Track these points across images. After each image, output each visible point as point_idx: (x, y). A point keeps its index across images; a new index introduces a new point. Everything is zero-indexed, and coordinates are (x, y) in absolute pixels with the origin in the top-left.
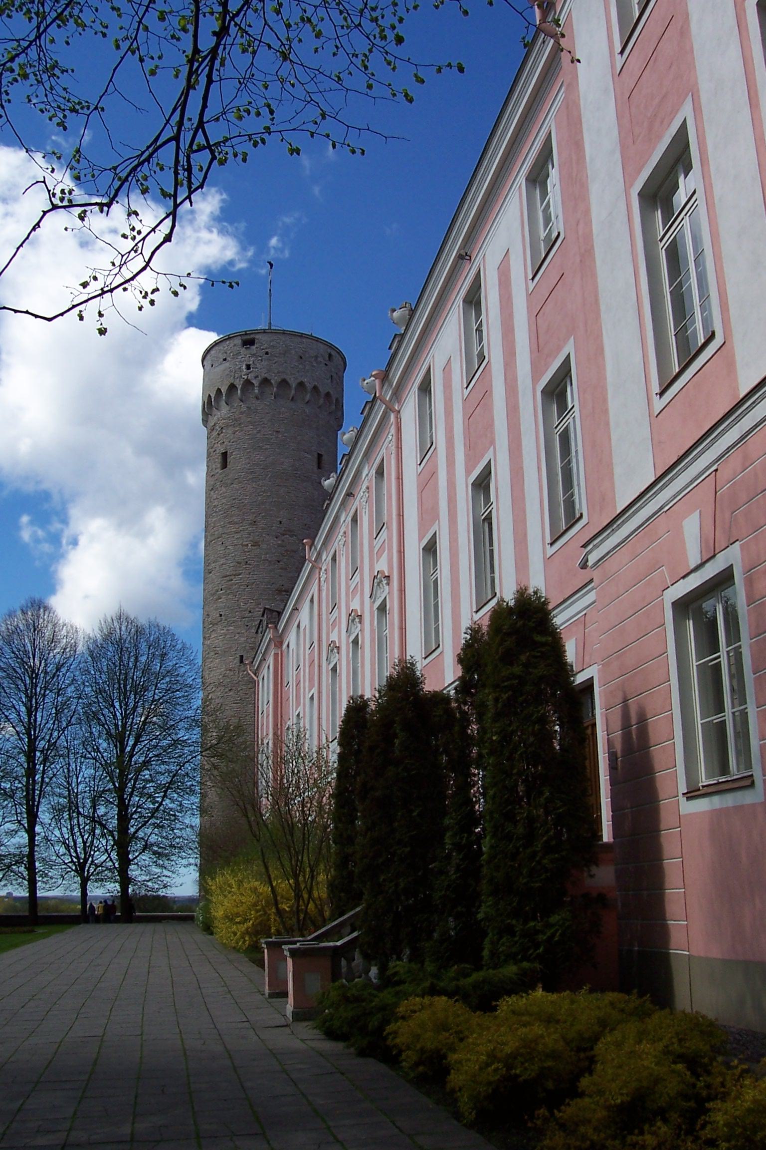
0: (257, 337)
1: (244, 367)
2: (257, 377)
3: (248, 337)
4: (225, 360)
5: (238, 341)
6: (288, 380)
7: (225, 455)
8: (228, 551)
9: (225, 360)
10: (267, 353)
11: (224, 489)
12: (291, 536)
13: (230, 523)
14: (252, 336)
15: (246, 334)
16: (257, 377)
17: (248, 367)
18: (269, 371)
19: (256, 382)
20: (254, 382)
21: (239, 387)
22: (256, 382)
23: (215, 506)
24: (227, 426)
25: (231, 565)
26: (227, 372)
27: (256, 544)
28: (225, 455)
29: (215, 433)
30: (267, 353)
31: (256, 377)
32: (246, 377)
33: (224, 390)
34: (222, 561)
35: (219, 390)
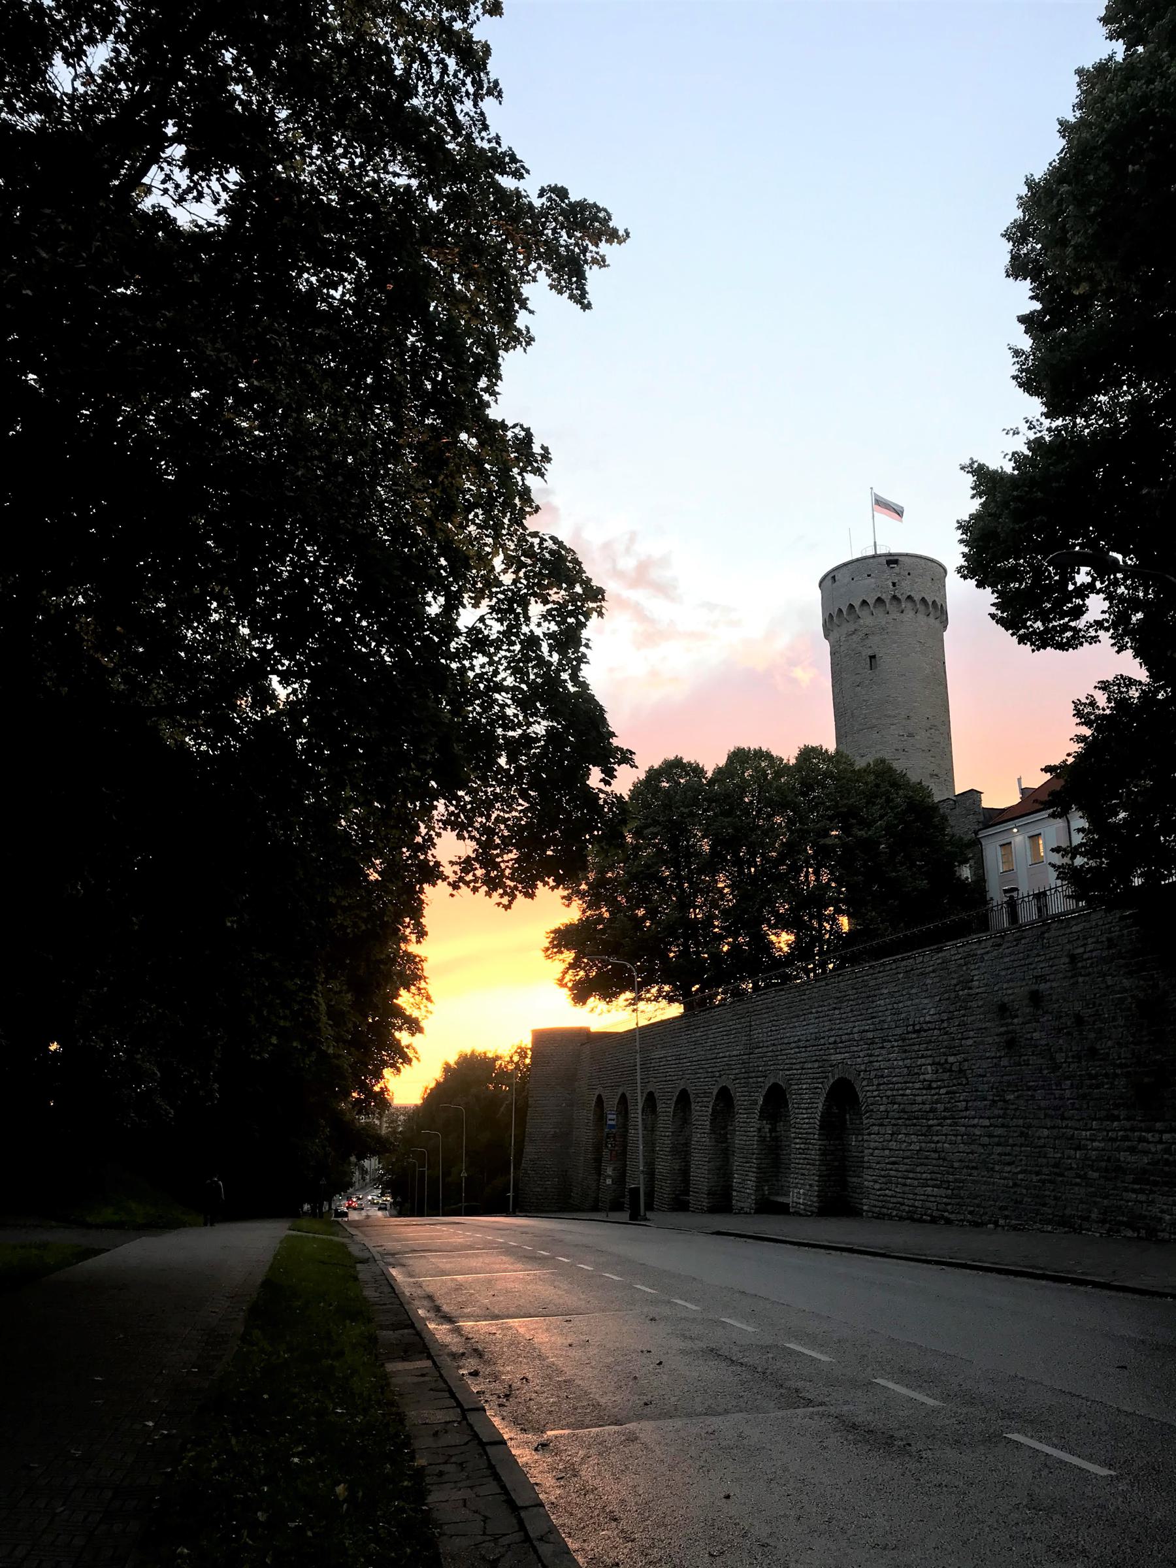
17: (894, 584)
19: (903, 598)
21: (887, 602)
33: (871, 601)
35: (864, 602)
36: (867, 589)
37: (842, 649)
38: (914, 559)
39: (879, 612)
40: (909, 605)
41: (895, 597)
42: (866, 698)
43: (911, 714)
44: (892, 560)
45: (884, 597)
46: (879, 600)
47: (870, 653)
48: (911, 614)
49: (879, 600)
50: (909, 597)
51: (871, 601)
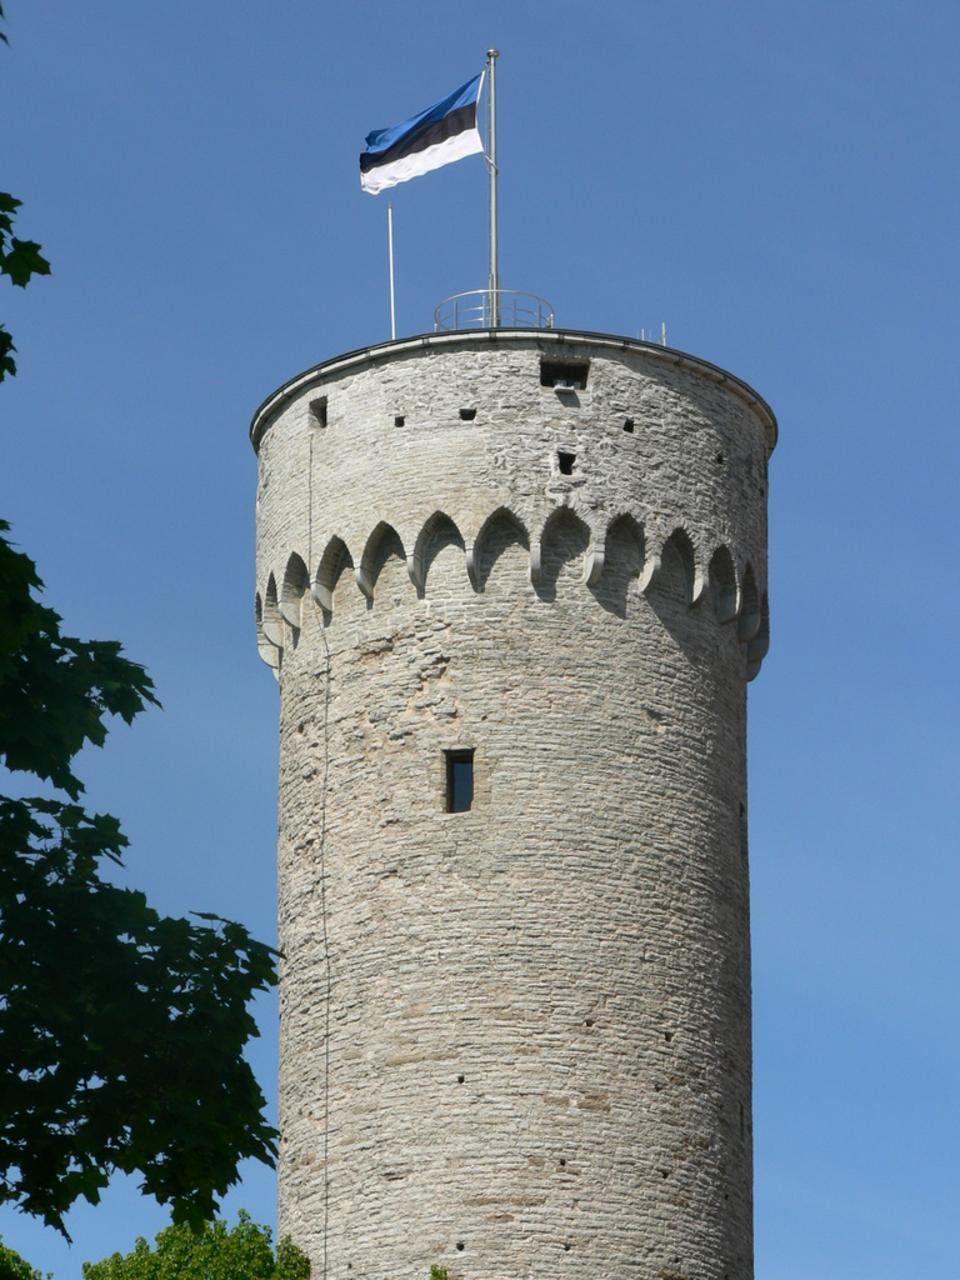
0: (597, 361)
1: (552, 460)
2: (596, 506)
4: (467, 415)
6: (691, 533)
7: (459, 763)
8: (486, 1112)
9: (467, 415)
11: (459, 885)
17: (566, 462)
18: (639, 491)
19: (597, 525)
22: (597, 525)
24: (471, 658)
25: (504, 1163)
27: (594, 1102)
28: (459, 763)
29: (395, 669)
30: (629, 426)
31: (596, 506)
32: (560, 498)
33: (470, 524)
34: (462, 1144)
37: (335, 712)
42: (420, 926)
47: (453, 740)
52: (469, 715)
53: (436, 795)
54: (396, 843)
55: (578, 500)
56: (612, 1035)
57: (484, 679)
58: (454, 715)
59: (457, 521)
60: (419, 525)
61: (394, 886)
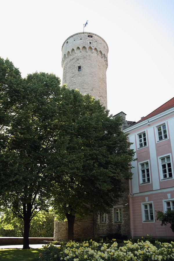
1: (89, 43)
3: (90, 35)
5: (87, 35)
7: (80, 68)
10: (96, 41)
12: (103, 98)
13: (83, 88)
14: (92, 35)
15: (90, 34)
16: (93, 47)
17: (90, 43)
20: (92, 47)
21: (87, 48)
23: (74, 83)
26: (82, 43)
28: (80, 68)
29: (73, 61)
30: (96, 41)
35: (78, 48)
36: (79, 43)
38: (98, 37)
39: (83, 52)
40: (95, 52)
41: (90, 48)
42: (75, 81)
43: (93, 89)
44: (90, 36)
45: (86, 46)
46: (84, 47)
47: (79, 65)
48: (96, 55)
49: (84, 47)
50: (96, 49)
51: (81, 47)
52: (80, 63)
53: (77, 70)
54: (73, 75)
55: (91, 46)
56: (94, 91)
57: (82, 60)
58: (79, 63)
59: (80, 48)
60: (76, 48)
61: (72, 78)
